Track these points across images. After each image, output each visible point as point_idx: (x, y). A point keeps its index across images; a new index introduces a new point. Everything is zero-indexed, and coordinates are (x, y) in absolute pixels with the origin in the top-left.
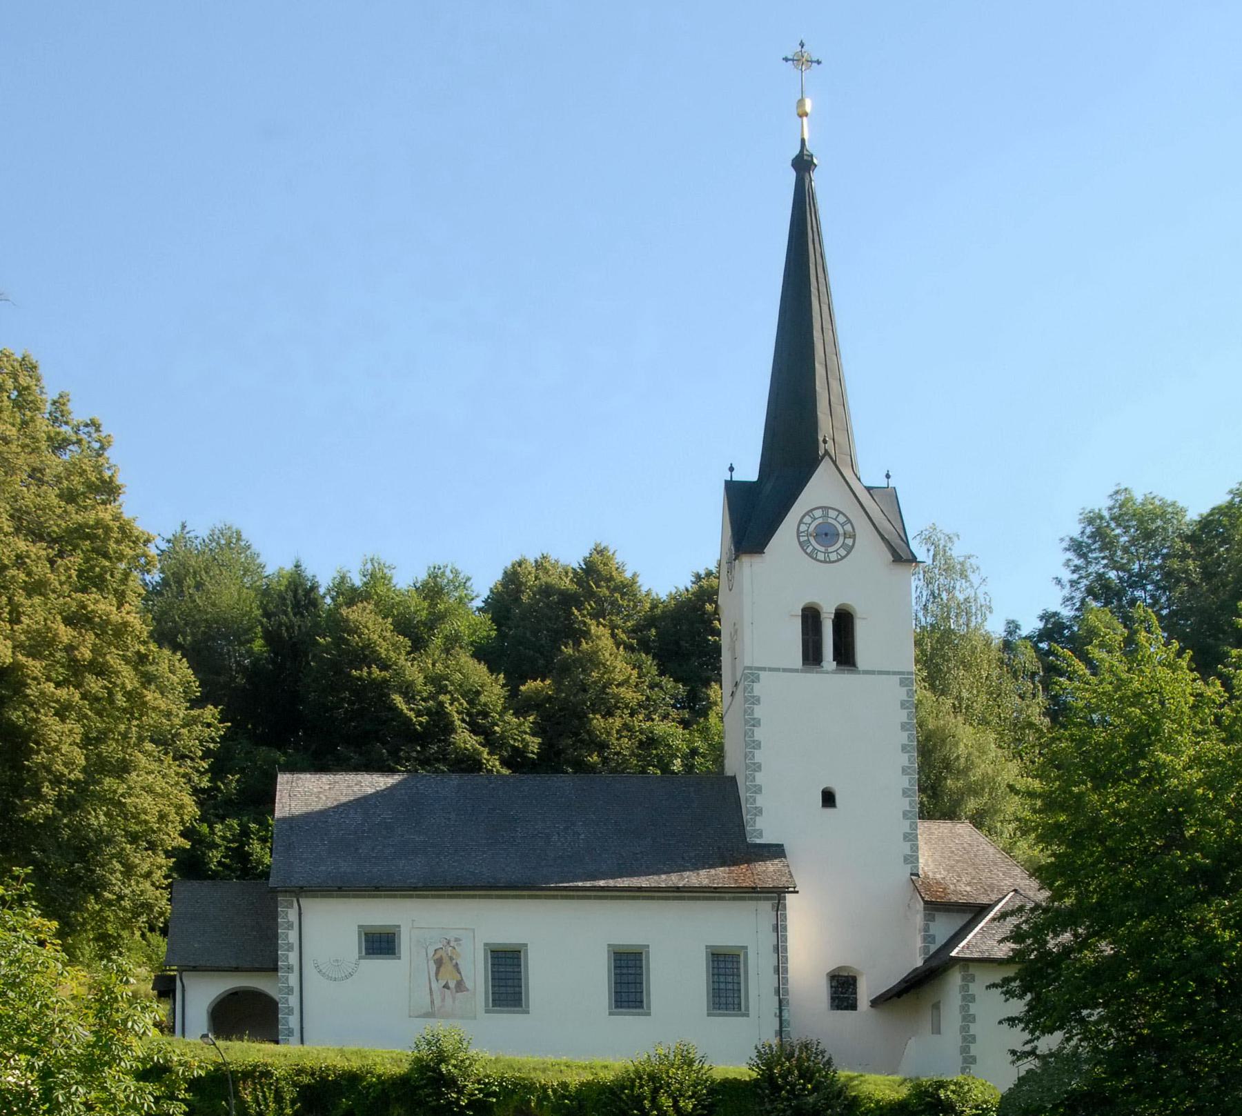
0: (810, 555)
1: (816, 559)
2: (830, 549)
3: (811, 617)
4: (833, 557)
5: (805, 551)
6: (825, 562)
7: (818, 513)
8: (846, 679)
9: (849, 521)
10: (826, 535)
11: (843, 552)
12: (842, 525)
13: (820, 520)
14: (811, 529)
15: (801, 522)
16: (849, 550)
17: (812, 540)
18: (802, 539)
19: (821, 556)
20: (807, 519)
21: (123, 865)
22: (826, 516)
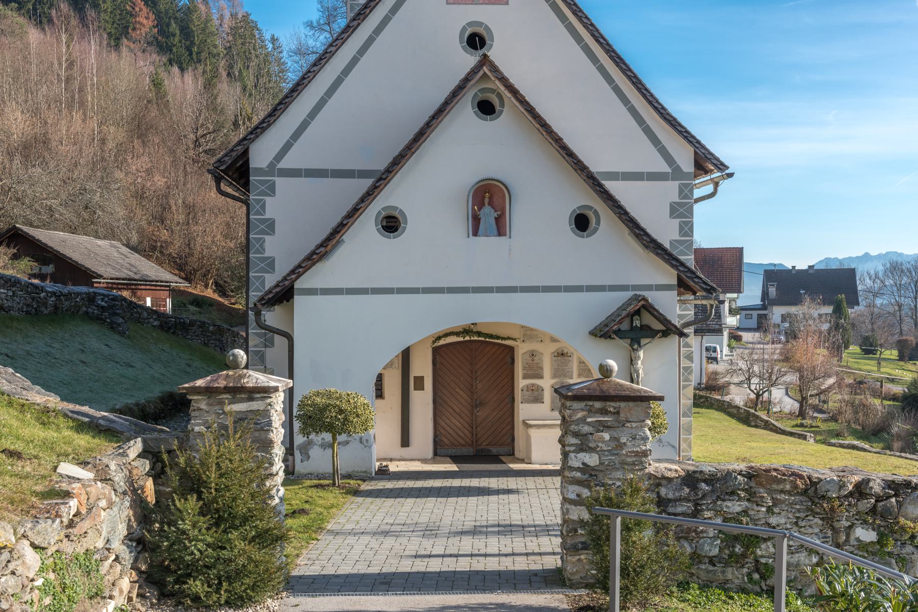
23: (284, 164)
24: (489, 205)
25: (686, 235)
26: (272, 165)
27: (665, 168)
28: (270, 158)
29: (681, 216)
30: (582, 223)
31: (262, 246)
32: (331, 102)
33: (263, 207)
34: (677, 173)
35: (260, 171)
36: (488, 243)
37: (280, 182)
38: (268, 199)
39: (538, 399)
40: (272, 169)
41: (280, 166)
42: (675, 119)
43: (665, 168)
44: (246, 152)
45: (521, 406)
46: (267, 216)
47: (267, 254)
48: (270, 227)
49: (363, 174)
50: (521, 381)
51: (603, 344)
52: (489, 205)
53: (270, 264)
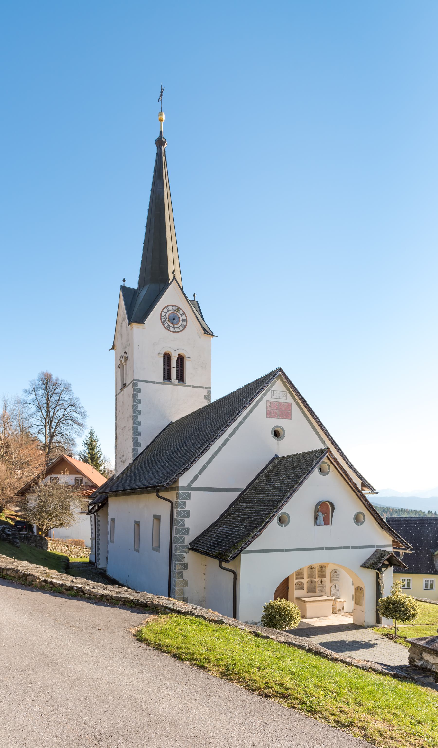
1: (169, 330)
2: (176, 326)
3: (167, 358)
4: (177, 330)
5: (164, 326)
6: (173, 332)
7: (171, 308)
8: (181, 389)
9: (184, 313)
10: (173, 319)
11: (181, 328)
12: (182, 315)
13: (172, 312)
14: (167, 316)
15: (162, 311)
16: (184, 327)
18: (163, 320)
19: (171, 329)
20: (165, 310)
21: (161, 149)
23: (194, 485)
26: (189, 485)
28: (188, 482)
31: (183, 523)
32: (216, 458)
33: (185, 505)
35: (183, 488)
37: (193, 493)
39: (302, 588)
40: (189, 487)
41: (193, 486)
42: (356, 470)
45: (295, 591)
46: (186, 509)
47: (186, 526)
48: (188, 514)
50: (295, 580)
53: (187, 531)
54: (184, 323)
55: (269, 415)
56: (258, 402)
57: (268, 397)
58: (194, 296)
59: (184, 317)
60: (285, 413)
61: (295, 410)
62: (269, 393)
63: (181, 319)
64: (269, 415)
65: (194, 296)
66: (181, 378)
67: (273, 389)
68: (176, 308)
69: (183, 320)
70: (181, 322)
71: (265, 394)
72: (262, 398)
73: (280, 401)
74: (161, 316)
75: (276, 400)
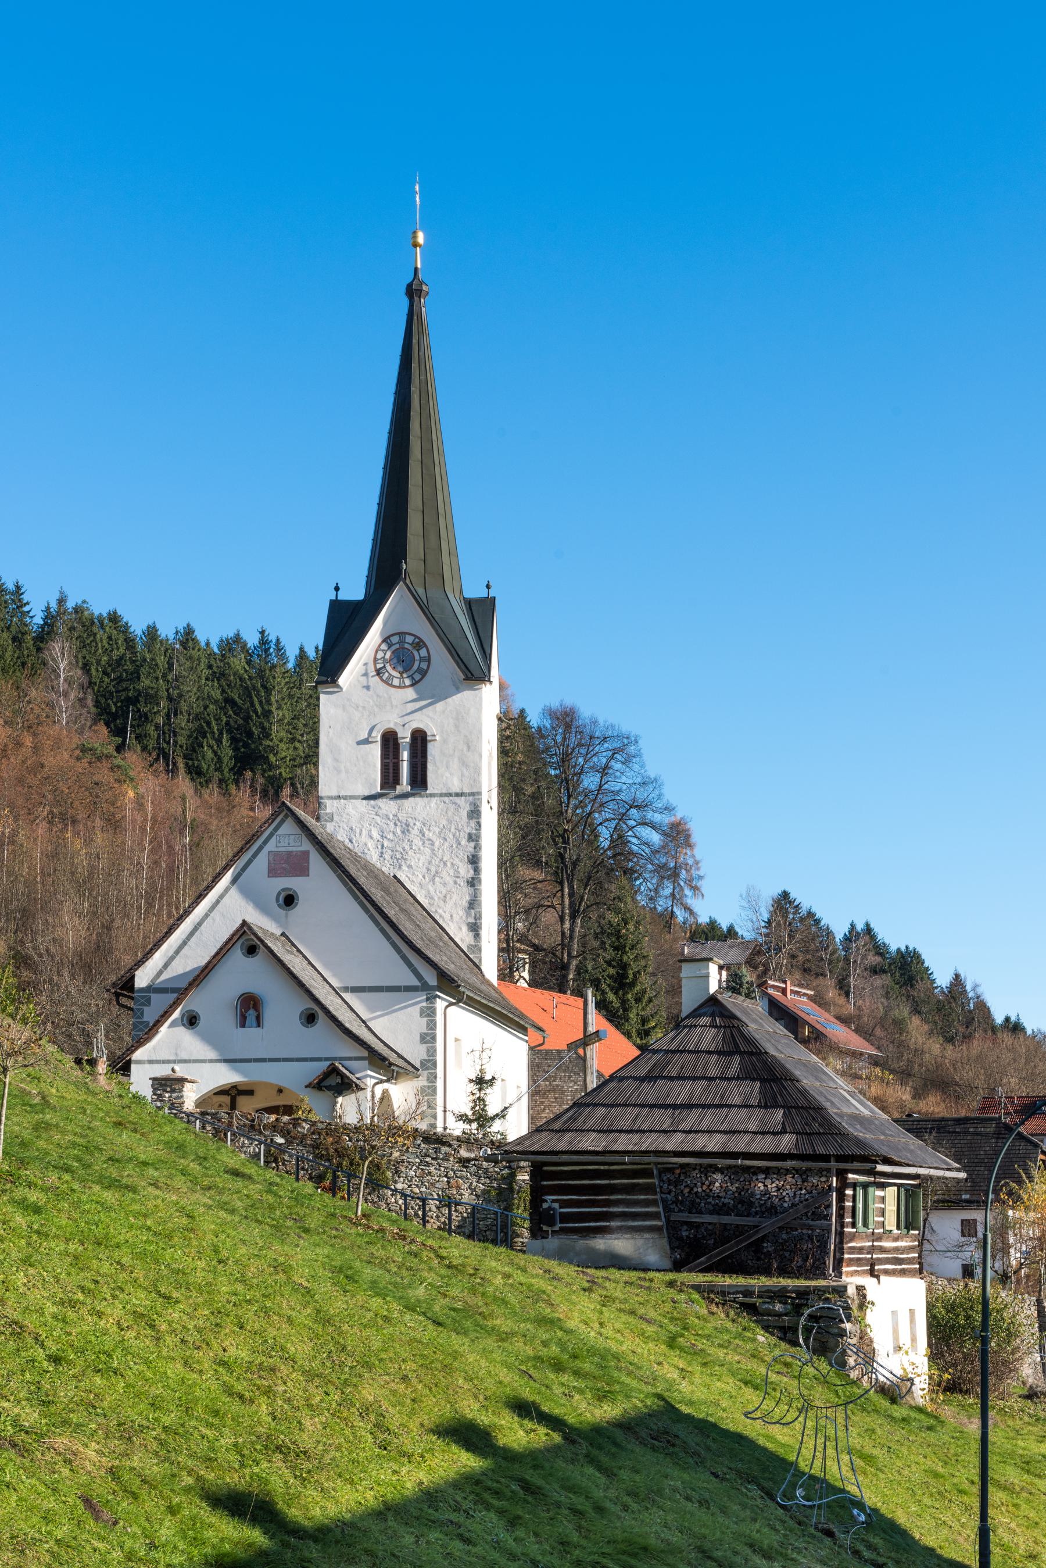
0: (386, 682)
6: (399, 687)
13: (397, 646)
17: (388, 668)
19: (396, 682)
22: (402, 642)
24: (250, 1008)
25: (432, 1029)
27: (416, 982)
29: (429, 1015)
30: (310, 1019)
33: (142, 1014)
34: (425, 987)
35: (142, 990)
36: (252, 1032)
37: (154, 997)
38: (145, 1008)
40: (149, 989)
43: (416, 982)
44: (133, 977)
46: (145, 1019)
49: (173, 990)
51: (320, 1094)
52: (250, 1008)
54: (424, 666)
55: (273, 872)
56: (255, 856)
57: (271, 846)
58: (488, 587)
59: (423, 652)
60: (297, 866)
61: (316, 862)
62: (273, 840)
63: (417, 657)
64: (273, 872)
65: (488, 587)
66: (419, 780)
67: (278, 833)
68: (409, 639)
69: (422, 659)
70: (417, 663)
71: (265, 842)
72: (260, 848)
73: (290, 849)
74: (375, 660)
75: (283, 849)
